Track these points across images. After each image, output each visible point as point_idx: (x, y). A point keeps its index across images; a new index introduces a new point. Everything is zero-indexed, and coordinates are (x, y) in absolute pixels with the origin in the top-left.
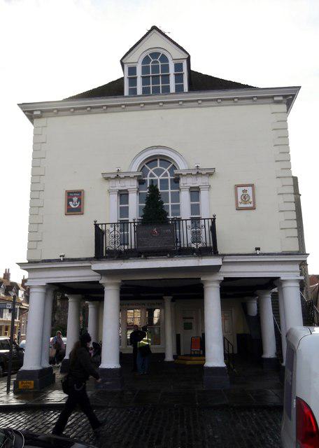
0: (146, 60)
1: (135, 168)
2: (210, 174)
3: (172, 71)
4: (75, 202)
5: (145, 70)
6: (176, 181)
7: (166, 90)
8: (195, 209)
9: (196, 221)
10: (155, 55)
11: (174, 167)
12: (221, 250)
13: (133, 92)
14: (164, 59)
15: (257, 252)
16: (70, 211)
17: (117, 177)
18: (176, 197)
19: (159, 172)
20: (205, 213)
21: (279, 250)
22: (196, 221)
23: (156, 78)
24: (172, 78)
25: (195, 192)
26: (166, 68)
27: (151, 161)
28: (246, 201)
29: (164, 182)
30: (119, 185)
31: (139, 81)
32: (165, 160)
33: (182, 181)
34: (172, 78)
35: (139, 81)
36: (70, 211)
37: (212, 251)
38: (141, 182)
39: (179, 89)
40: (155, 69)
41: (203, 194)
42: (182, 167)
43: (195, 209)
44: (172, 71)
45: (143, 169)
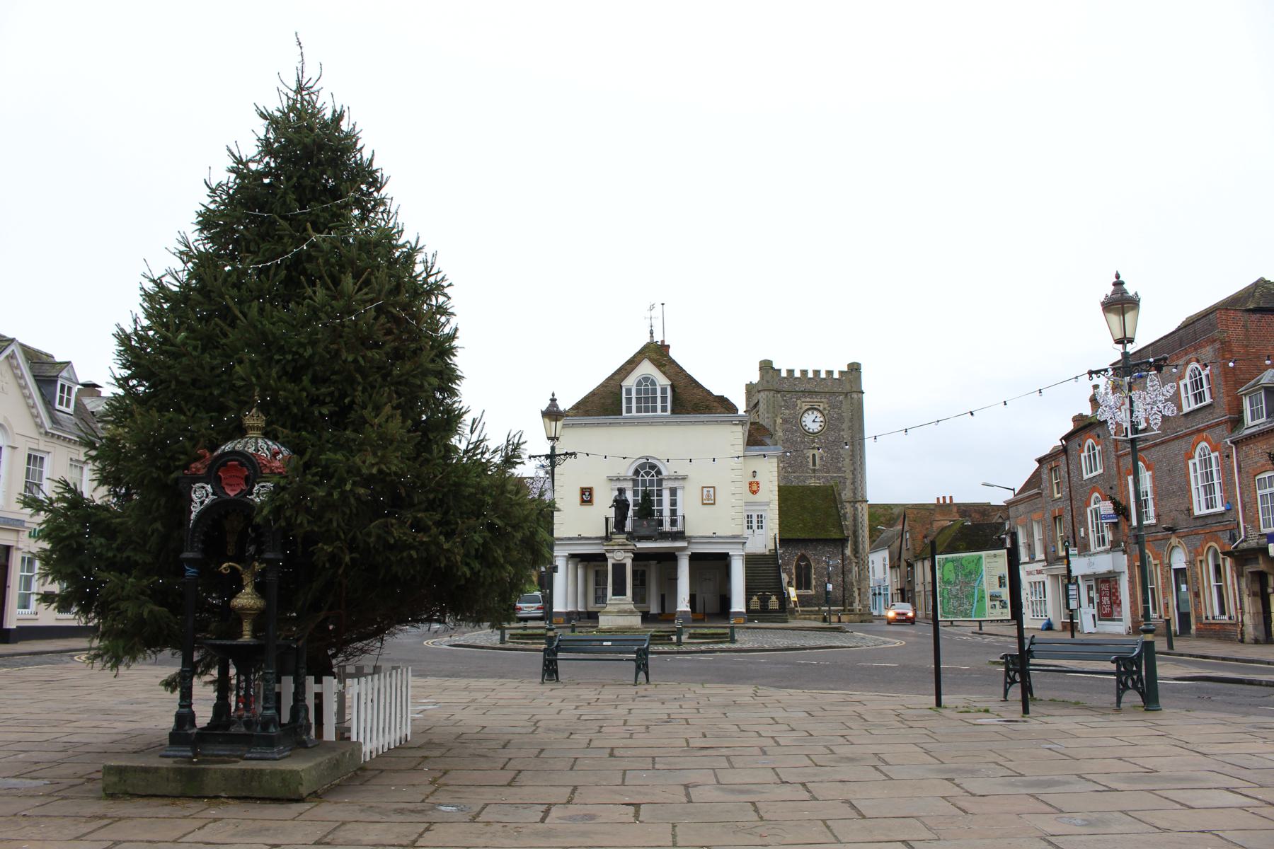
0: (639, 383)
1: (630, 473)
2: (684, 478)
3: (659, 394)
4: (587, 496)
5: (638, 392)
6: (660, 482)
7: (654, 410)
8: (674, 503)
9: (673, 512)
10: (646, 379)
11: (659, 473)
12: (687, 534)
13: (629, 410)
14: (653, 383)
15: (714, 536)
16: (583, 502)
17: (618, 479)
18: (659, 495)
19: (647, 473)
20: (679, 513)
21: (729, 534)
22: (673, 512)
23: (646, 400)
24: (659, 400)
25: (673, 492)
26: (654, 391)
27: (642, 466)
28: (709, 500)
29: (651, 482)
30: (620, 485)
31: (634, 401)
32: (653, 467)
33: (664, 483)
34: (659, 400)
35: (634, 401)
36: (583, 502)
37: (680, 536)
38: (635, 482)
39: (664, 409)
40: (646, 391)
41: (679, 493)
42: (665, 473)
43: (674, 503)
44: (659, 394)
45: (637, 472)
